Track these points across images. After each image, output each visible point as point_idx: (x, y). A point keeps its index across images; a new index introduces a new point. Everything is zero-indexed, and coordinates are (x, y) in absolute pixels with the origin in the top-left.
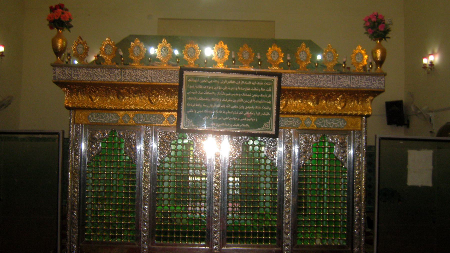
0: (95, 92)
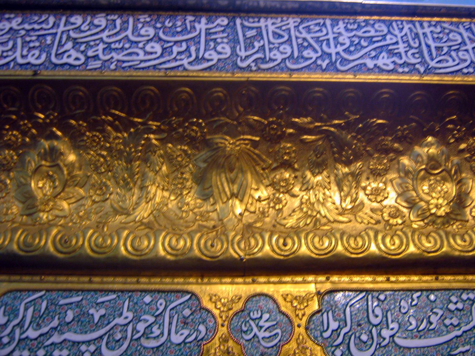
0: (53, 155)
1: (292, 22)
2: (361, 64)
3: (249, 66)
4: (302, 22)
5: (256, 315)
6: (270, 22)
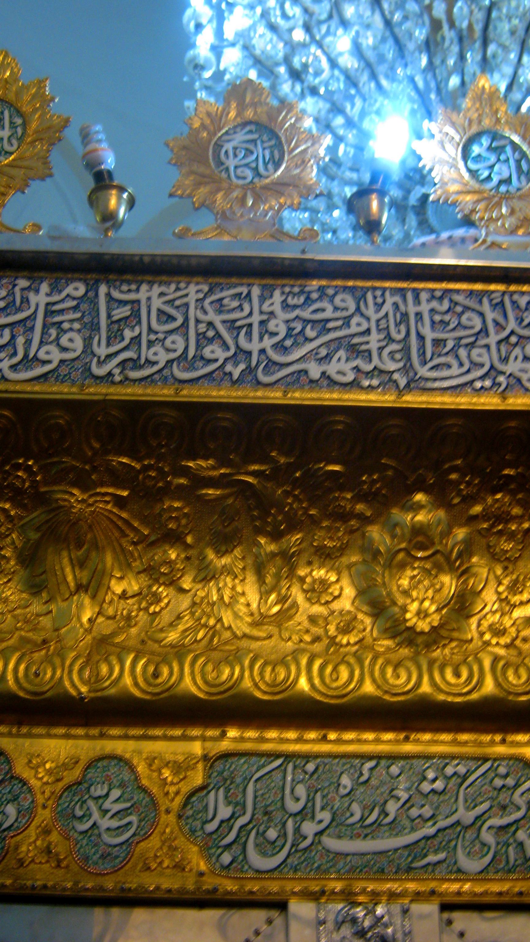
1: (193, 291)
2: (300, 371)
3: (110, 374)
4: (211, 291)
5: (99, 791)
6: (156, 290)
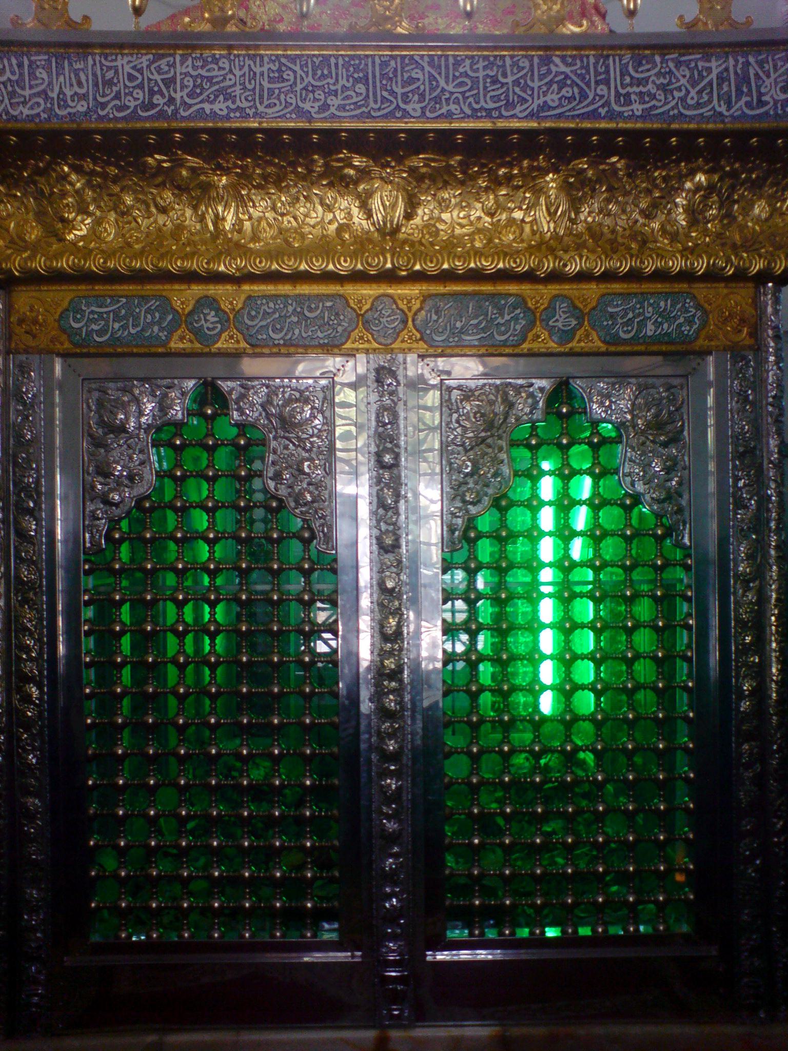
6: (126, 59)
